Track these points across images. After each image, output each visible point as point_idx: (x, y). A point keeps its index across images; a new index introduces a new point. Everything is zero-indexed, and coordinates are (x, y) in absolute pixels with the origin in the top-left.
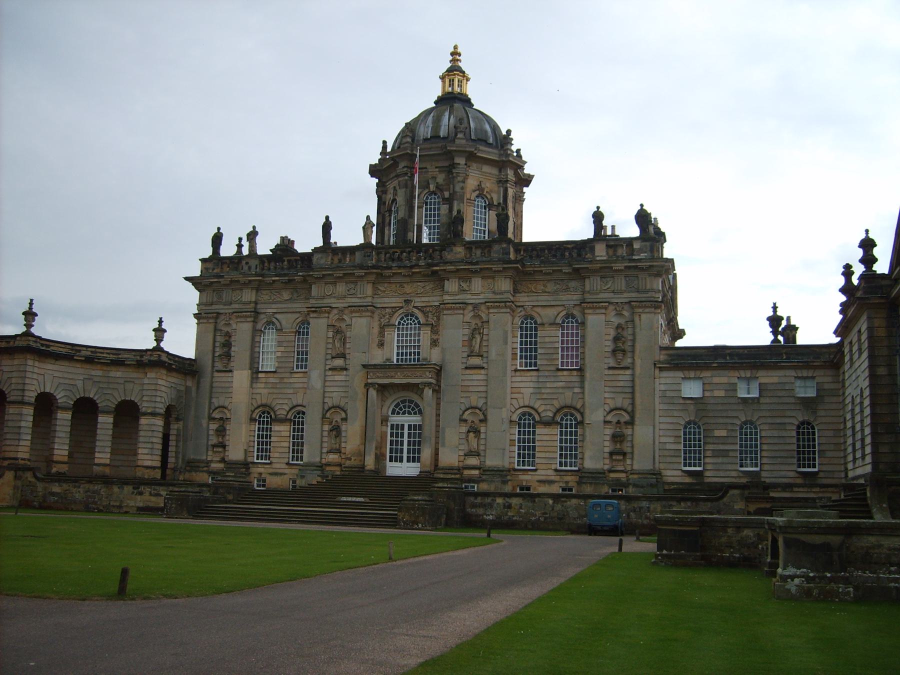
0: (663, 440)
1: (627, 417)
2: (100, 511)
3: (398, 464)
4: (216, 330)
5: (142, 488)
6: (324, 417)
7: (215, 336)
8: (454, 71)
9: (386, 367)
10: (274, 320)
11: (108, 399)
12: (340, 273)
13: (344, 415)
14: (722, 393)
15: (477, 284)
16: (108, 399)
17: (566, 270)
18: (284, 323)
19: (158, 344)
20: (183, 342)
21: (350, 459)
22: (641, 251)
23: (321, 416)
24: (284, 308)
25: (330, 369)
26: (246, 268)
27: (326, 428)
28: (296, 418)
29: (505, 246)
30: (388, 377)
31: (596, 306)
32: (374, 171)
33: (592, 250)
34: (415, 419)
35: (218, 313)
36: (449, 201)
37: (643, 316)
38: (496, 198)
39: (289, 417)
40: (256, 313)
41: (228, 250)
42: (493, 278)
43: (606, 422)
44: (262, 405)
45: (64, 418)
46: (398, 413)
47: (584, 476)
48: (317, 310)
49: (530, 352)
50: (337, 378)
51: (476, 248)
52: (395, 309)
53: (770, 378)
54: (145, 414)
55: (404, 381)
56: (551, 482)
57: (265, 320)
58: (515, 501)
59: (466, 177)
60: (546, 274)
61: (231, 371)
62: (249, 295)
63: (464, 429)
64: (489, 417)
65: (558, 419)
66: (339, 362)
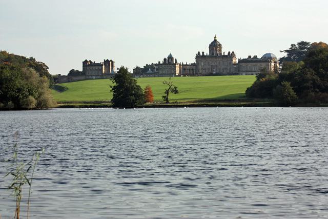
8: (215, 37)
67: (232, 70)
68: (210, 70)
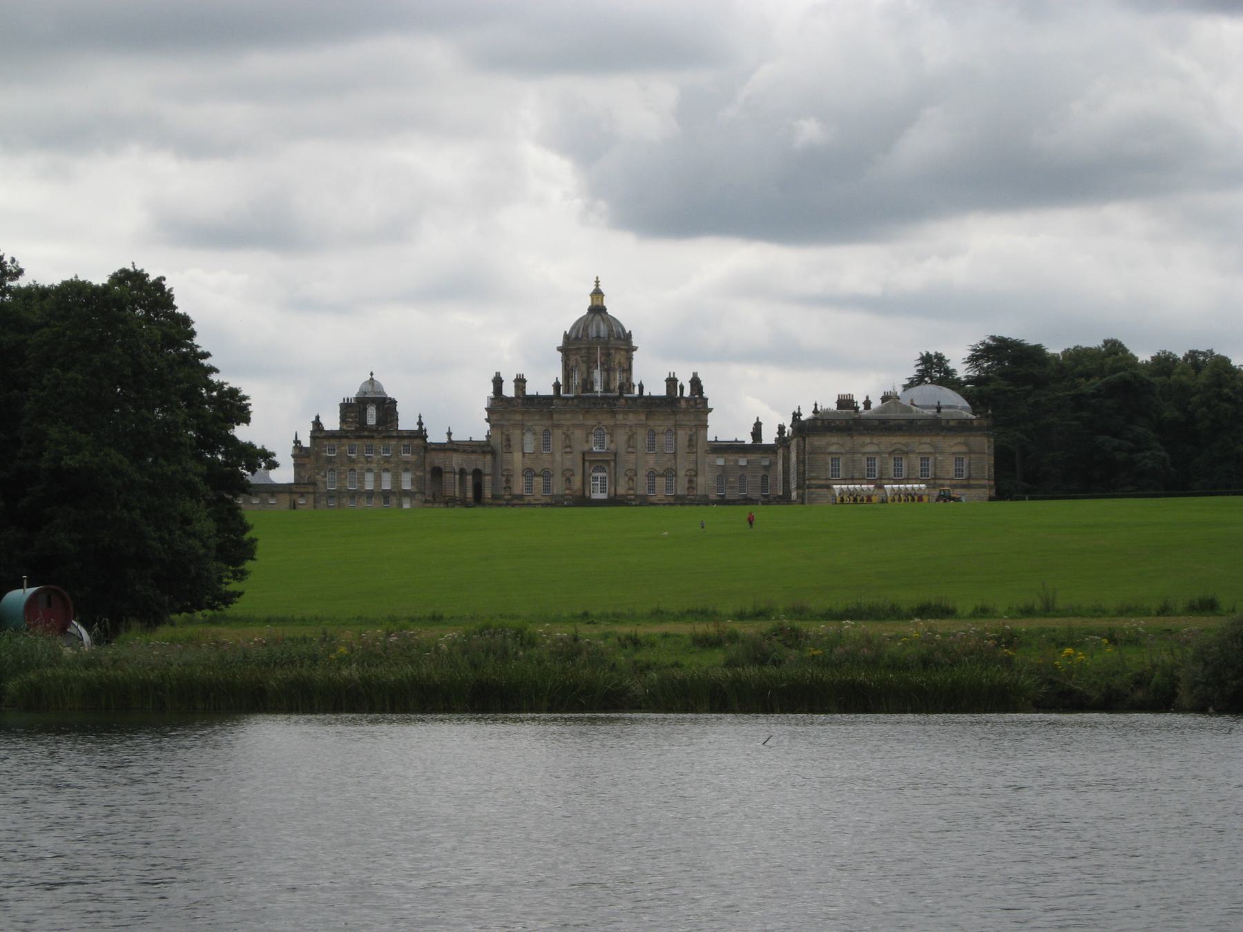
8: (597, 293)
11: (470, 469)
15: (631, 416)
28: (547, 475)
31: (682, 426)
34: (604, 475)
48: (558, 426)
49: (651, 446)
53: (752, 457)
62: (518, 417)
66: (568, 450)
67: (701, 480)
68: (577, 482)
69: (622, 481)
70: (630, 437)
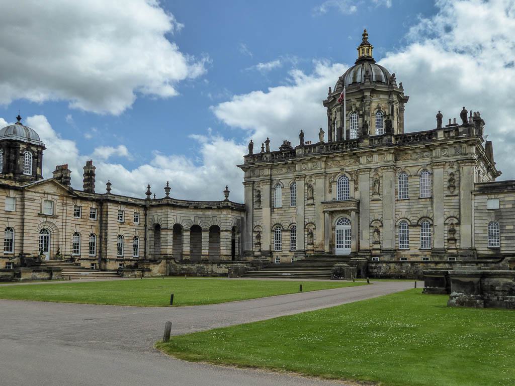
0: (477, 232)
1: (456, 221)
2: (204, 276)
3: (341, 249)
4: (253, 189)
5: (221, 265)
6: (305, 228)
7: (253, 192)
9: (334, 202)
10: (280, 183)
11: (205, 225)
12: (309, 158)
13: (314, 227)
14: (510, 206)
15: (376, 157)
16: (205, 225)
17: (422, 146)
18: (284, 184)
19: (227, 198)
20: (239, 195)
21: (318, 248)
22: (463, 133)
23: (303, 228)
24: (284, 176)
25: (307, 205)
26: (265, 159)
27: (306, 233)
28: (292, 230)
29: (389, 137)
30: (333, 207)
31: (438, 164)
32: (326, 104)
33: (436, 135)
34: (348, 227)
35: (254, 182)
36: (362, 116)
37: (465, 168)
38: (388, 111)
39: (289, 229)
40: (271, 181)
41: (257, 150)
42: (384, 154)
43: (445, 224)
44: (276, 224)
45: (186, 235)
46: (340, 224)
47: (435, 252)
48: (299, 177)
50: (310, 209)
51: (375, 139)
52: (336, 174)
54: (222, 231)
55: (342, 209)
56: (417, 256)
57: (276, 183)
58: (392, 265)
59: (371, 102)
60: (411, 150)
61: (261, 209)
62: (267, 172)
63: (372, 231)
64: (384, 224)
65: (420, 223)
66: (311, 201)
67: (464, 230)
69: (366, 233)
70: (376, 182)
